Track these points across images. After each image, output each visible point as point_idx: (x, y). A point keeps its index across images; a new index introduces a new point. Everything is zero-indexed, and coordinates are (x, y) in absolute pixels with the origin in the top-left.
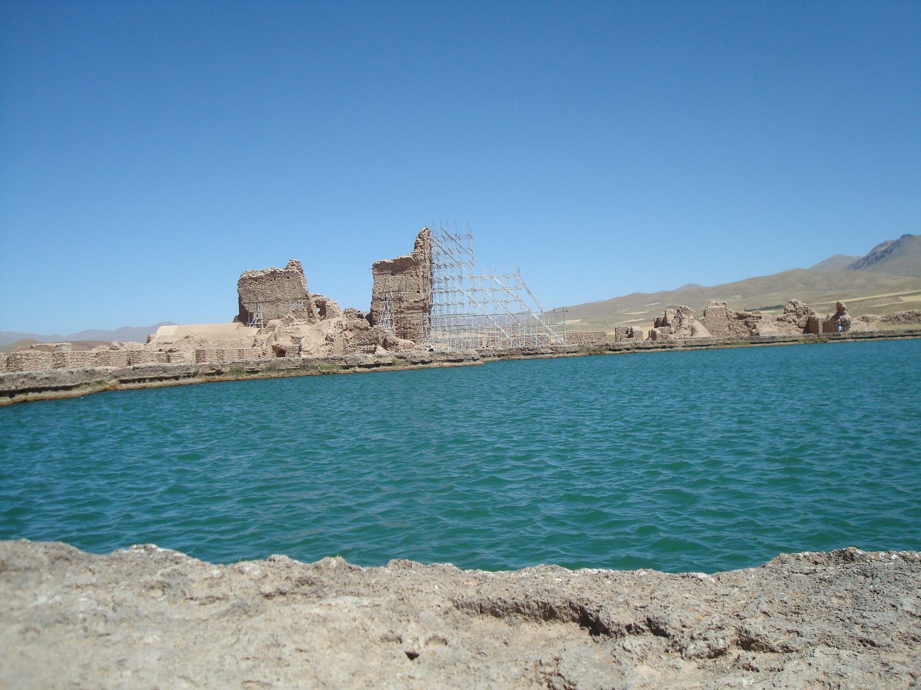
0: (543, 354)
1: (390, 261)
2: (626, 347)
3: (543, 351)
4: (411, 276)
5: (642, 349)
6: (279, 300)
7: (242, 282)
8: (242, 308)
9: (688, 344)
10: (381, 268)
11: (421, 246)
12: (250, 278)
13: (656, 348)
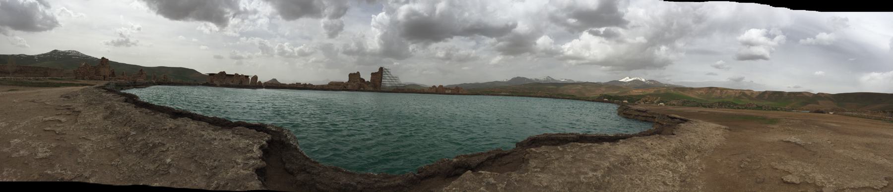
10: (372, 74)
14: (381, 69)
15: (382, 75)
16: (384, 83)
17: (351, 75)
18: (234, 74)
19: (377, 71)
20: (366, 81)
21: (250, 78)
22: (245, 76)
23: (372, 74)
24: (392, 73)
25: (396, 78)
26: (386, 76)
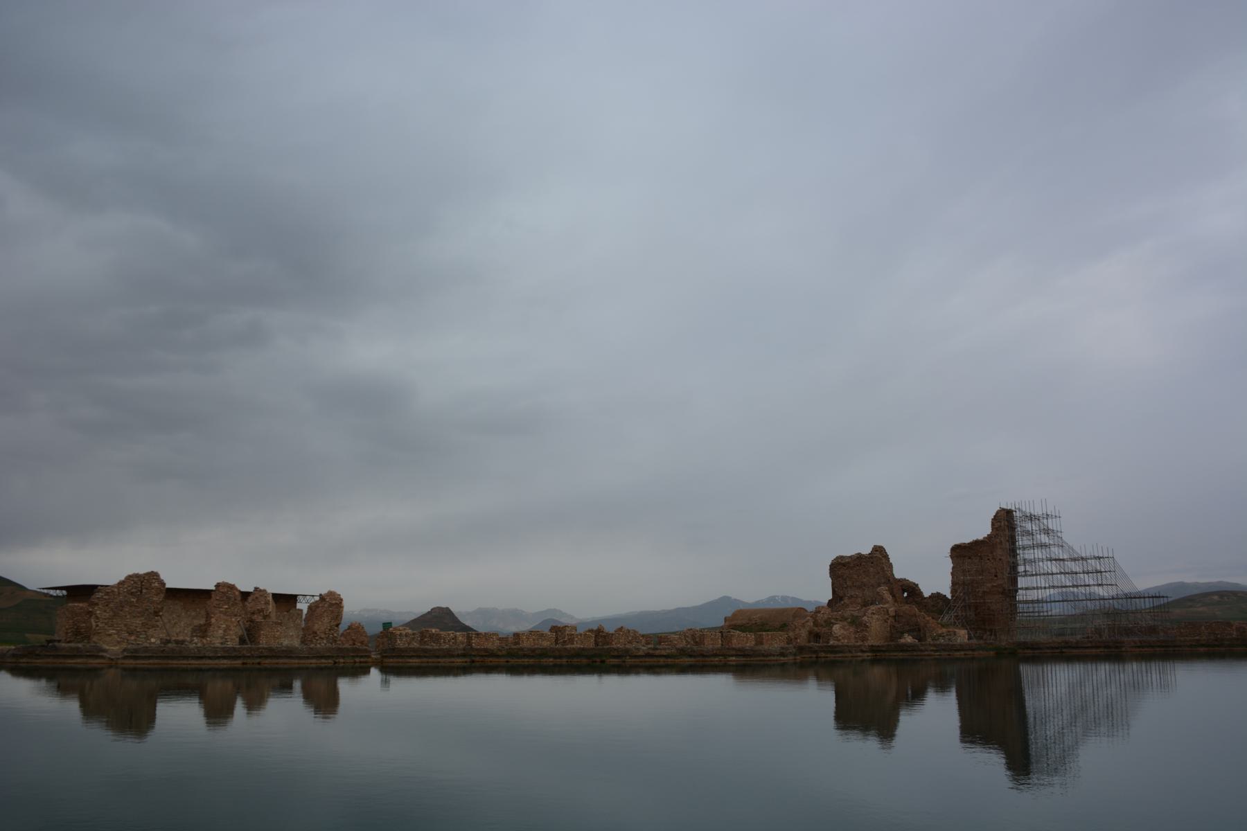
2: (1048, 646)
3: (923, 648)
4: (989, 559)
5: (1073, 648)
10: (959, 552)
12: (840, 564)
14: (1005, 521)
15: (1013, 552)
16: (1033, 595)
17: (841, 569)
18: (211, 586)
19: (981, 529)
20: (927, 594)
21: (303, 606)
22: (278, 598)
23: (959, 552)
24: (1067, 538)
25: (1098, 565)
26: (1038, 554)
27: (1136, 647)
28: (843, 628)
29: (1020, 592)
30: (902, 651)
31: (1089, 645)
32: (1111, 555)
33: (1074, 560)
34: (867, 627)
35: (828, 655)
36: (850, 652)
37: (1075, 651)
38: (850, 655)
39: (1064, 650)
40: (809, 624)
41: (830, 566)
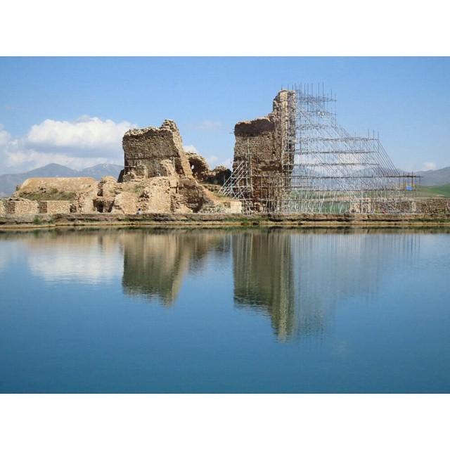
0: (173, 220)
1: (249, 122)
2: (288, 218)
3: (174, 218)
5: (311, 220)
6: (155, 157)
7: (126, 138)
8: (126, 163)
9: (371, 218)
10: (243, 131)
11: (277, 109)
12: (132, 136)
13: (331, 220)
27: (364, 220)
28: (126, 198)
29: (295, 167)
30: (156, 220)
31: (325, 218)
32: (376, 137)
33: (346, 140)
34: (148, 197)
35: (85, 223)
36: (106, 220)
37: (312, 224)
38: (107, 223)
39: (303, 222)
40: (93, 193)
41: (124, 138)
